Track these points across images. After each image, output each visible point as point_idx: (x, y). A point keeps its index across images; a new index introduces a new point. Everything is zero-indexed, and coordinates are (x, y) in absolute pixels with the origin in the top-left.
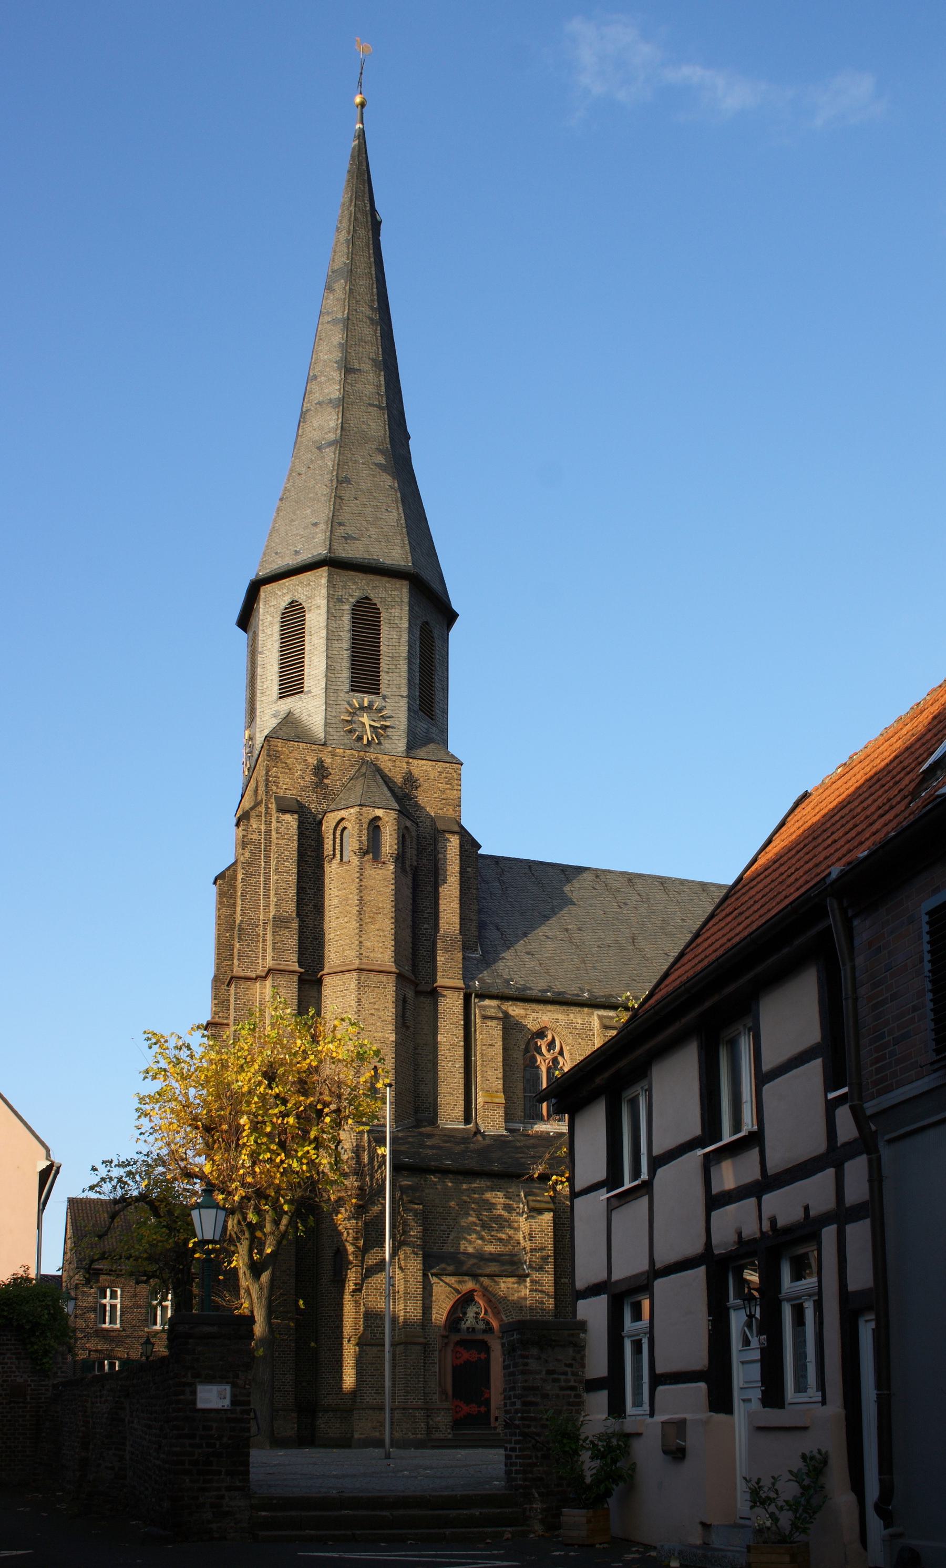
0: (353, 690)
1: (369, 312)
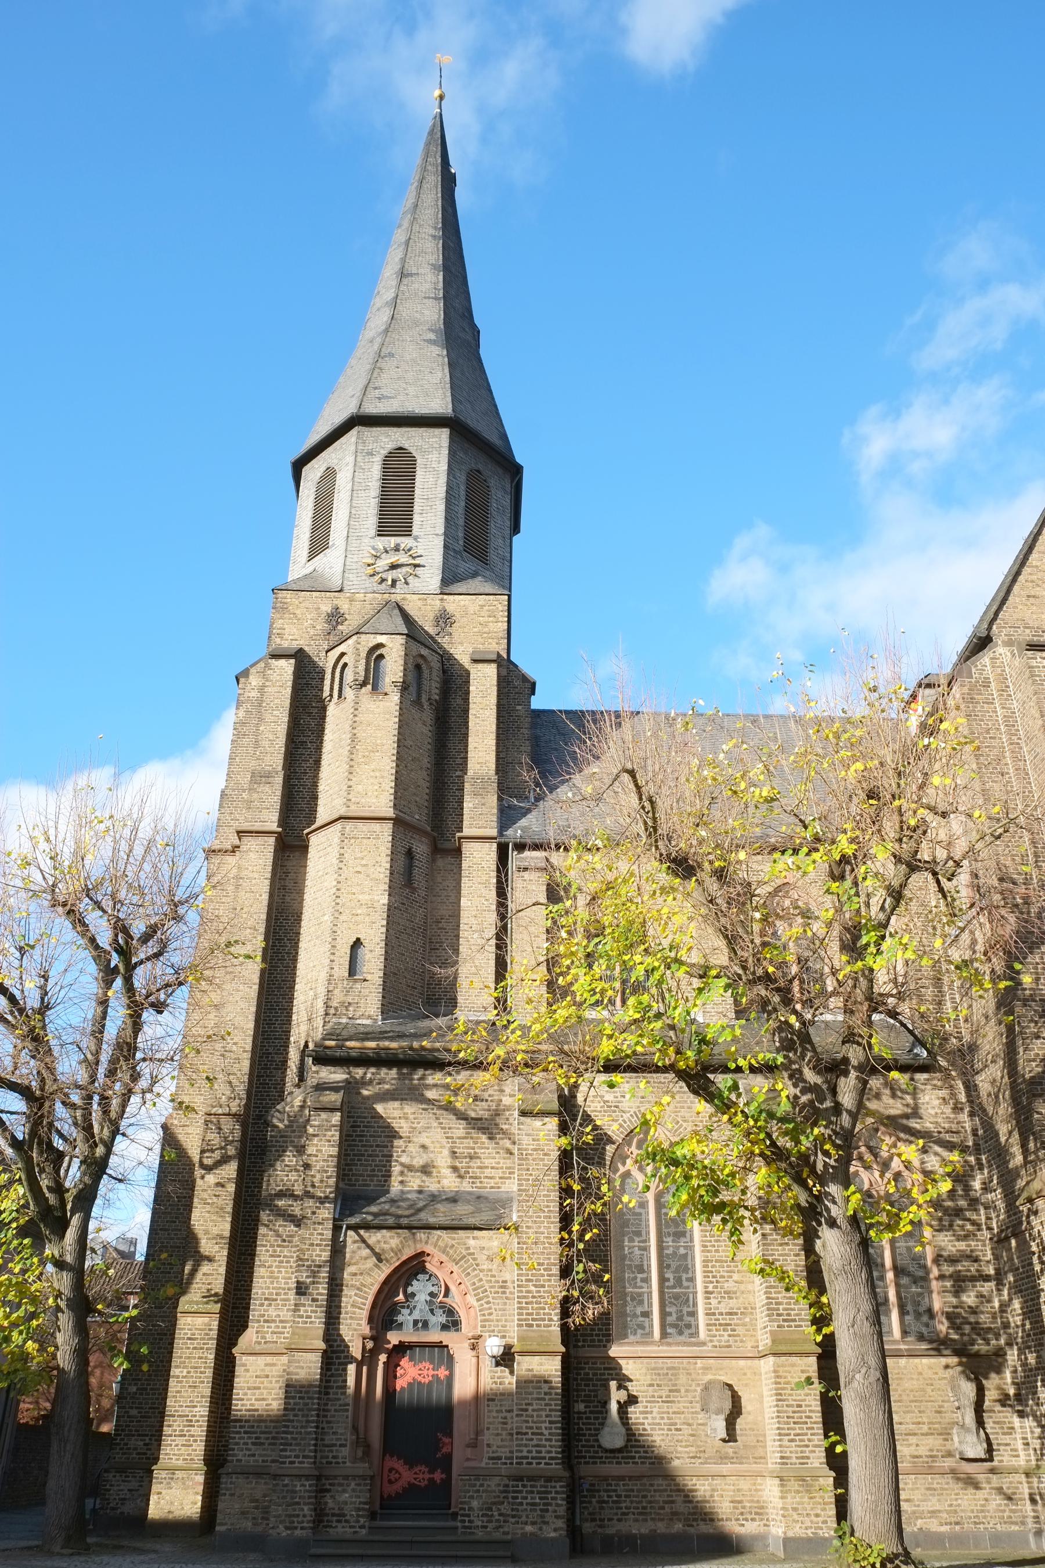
0: (379, 535)
1: (432, 232)
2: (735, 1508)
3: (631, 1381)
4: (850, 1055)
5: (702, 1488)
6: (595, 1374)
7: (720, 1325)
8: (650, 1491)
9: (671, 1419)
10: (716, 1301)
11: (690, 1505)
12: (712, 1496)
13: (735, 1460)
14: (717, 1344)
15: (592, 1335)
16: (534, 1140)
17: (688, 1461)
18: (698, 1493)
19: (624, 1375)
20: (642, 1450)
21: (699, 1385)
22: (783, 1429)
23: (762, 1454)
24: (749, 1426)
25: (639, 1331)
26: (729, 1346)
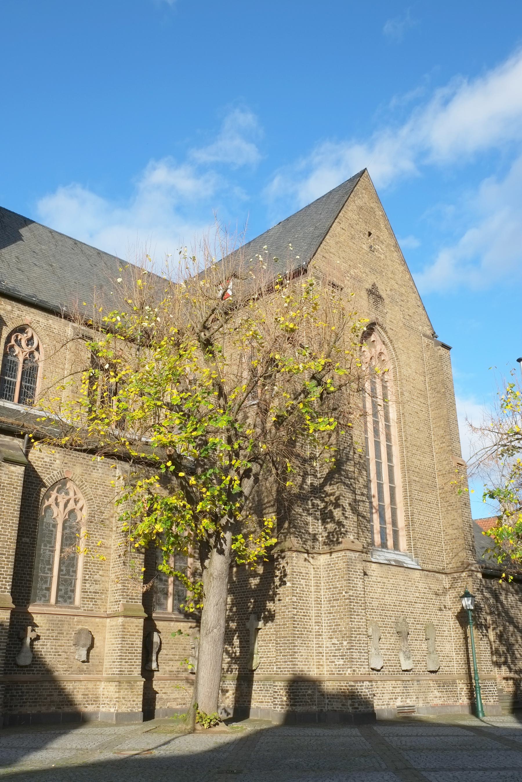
2: (84, 698)
3: (38, 626)
4: (253, 468)
5: (69, 687)
6: (17, 622)
7: (89, 598)
8: (40, 689)
9: (57, 649)
10: (89, 585)
11: (61, 697)
12: (73, 692)
13: (86, 672)
14: (86, 608)
15: (19, 599)
16: (9, 478)
17: (62, 672)
18: (66, 690)
19: (34, 623)
20: (38, 666)
21: (73, 631)
22: (123, 656)
23: (101, 669)
24: (97, 654)
25: (43, 599)
26: (92, 610)
